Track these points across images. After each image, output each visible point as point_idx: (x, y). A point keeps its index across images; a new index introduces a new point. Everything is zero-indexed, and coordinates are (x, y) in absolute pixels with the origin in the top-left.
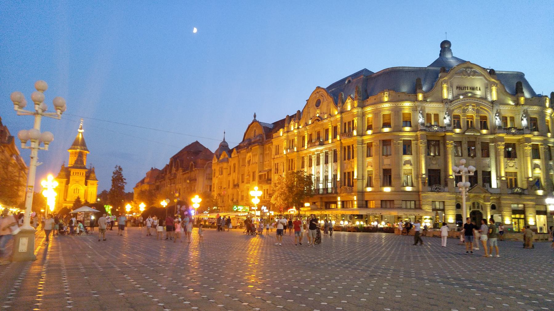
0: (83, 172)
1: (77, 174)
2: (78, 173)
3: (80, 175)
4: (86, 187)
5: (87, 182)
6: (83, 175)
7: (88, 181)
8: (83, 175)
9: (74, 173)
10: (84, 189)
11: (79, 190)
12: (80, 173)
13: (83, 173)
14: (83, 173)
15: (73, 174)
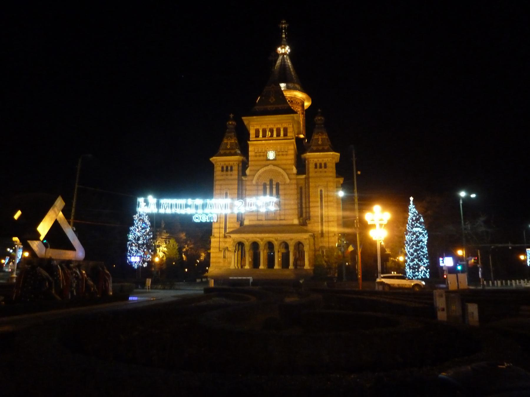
0: (285, 125)
1: (268, 134)
2: (272, 131)
3: (278, 135)
4: (303, 176)
5: (305, 159)
6: (285, 135)
7: (308, 155)
8: (285, 135)
9: (257, 132)
10: (294, 182)
11: (278, 185)
12: (278, 130)
13: (286, 130)
14: (286, 130)
15: (257, 136)
